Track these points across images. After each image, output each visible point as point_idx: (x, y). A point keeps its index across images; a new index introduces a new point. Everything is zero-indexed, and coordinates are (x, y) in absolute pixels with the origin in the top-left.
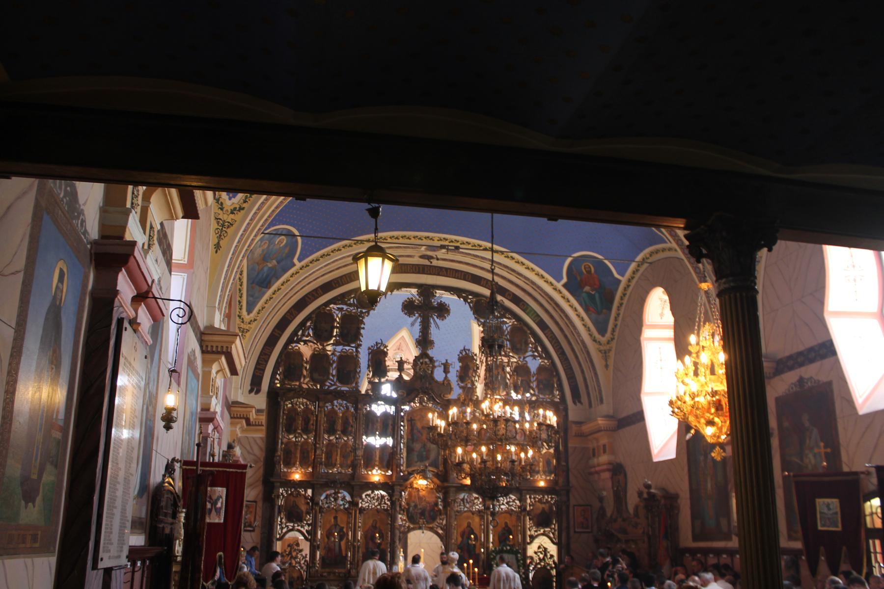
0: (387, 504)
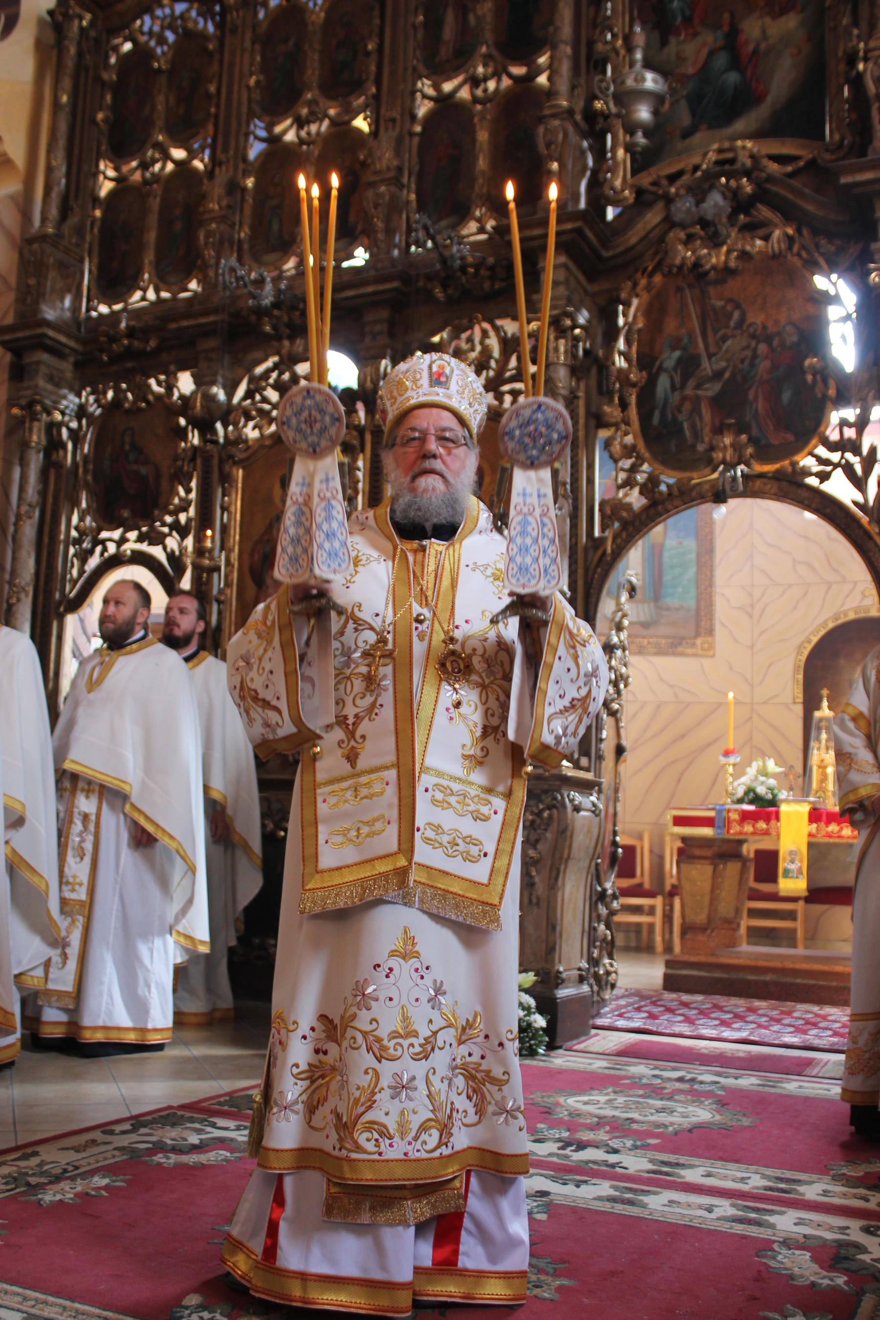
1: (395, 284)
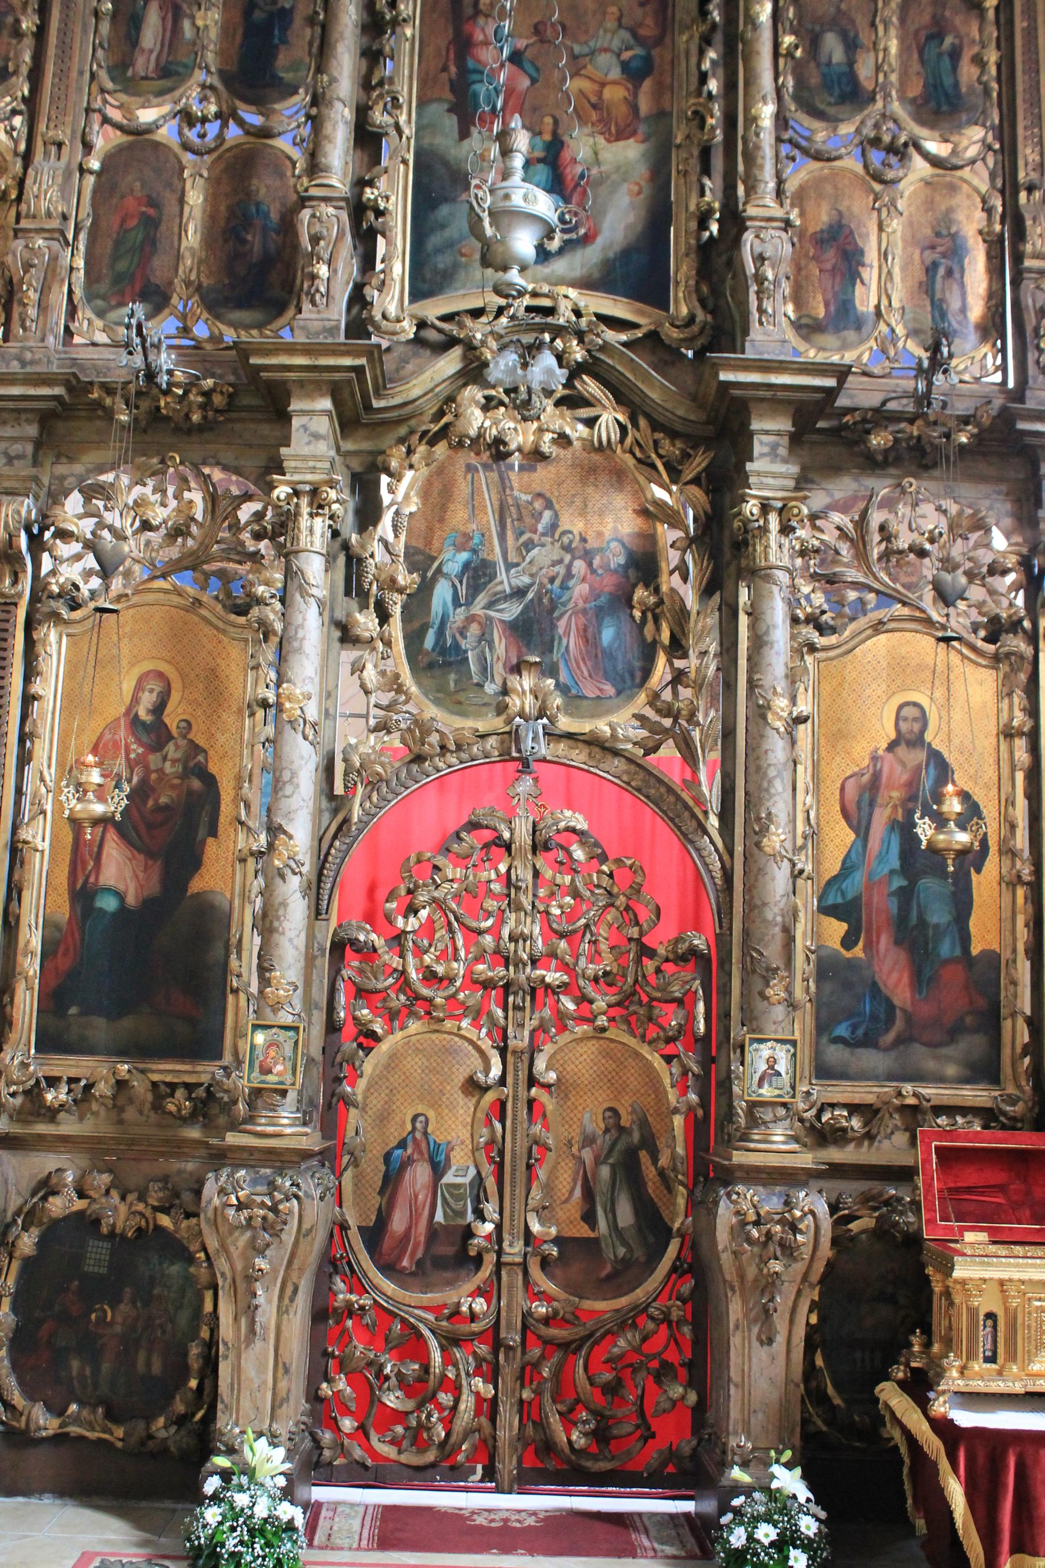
0: (255, 557)
1: (58, 391)
